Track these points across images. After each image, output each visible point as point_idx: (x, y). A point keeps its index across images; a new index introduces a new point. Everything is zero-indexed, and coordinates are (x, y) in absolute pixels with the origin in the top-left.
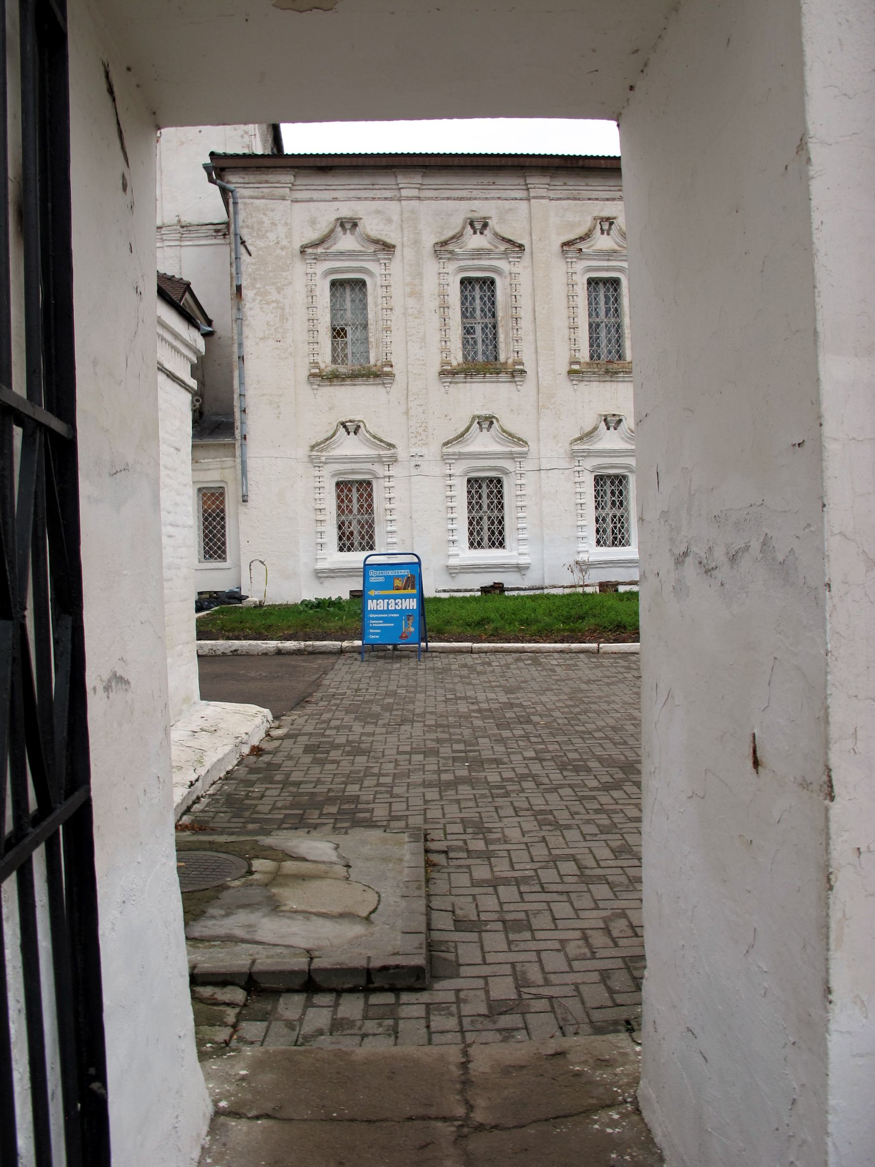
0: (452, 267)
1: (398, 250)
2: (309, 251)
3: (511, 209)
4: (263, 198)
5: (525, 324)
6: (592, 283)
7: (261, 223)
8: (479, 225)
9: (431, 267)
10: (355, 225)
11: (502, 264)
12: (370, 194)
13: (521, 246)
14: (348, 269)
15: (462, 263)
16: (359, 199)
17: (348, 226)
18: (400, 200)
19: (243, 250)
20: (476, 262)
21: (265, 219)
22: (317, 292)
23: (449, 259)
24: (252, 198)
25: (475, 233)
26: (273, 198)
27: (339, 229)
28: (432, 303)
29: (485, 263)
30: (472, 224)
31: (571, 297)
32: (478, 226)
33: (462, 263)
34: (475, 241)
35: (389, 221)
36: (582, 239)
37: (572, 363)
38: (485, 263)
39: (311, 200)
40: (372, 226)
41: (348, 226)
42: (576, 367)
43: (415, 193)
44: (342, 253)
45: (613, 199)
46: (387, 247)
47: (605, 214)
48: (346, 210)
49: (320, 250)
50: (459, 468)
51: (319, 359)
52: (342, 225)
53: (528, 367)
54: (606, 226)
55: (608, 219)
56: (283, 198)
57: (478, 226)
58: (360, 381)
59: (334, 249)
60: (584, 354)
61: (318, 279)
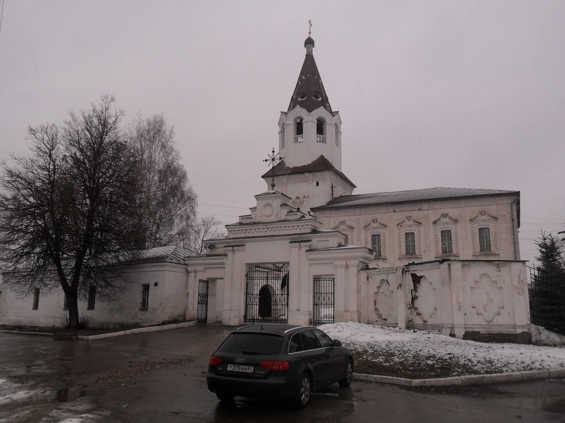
1: (355, 229)
4: (323, 217)
5: (387, 246)
8: (375, 221)
9: (363, 232)
10: (344, 223)
11: (381, 231)
12: (348, 214)
13: (386, 226)
15: (371, 231)
17: (343, 223)
18: (355, 215)
20: (375, 231)
25: (374, 223)
26: (325, 217)
27: (341, 224)
29: (377, 231)
30: (373, 221)
31: (400, 238)
32: (375, 221)
33: (371, 231)
34: (375, 225)
36: (402, 223)
38: (377, 231)
39: (334, 217)
40: (349, 223)
41: (343, 223)
42: (400, 257)
43: (359, 214)
46: (352, 228)
47: (409, 215)
48: (342, 219)
52: (341, 223)
53: (388, 258)
54: (409, 218)
55: (409, 217)
56: (328, 217)
57: (375, 221)
60: (404, 252)
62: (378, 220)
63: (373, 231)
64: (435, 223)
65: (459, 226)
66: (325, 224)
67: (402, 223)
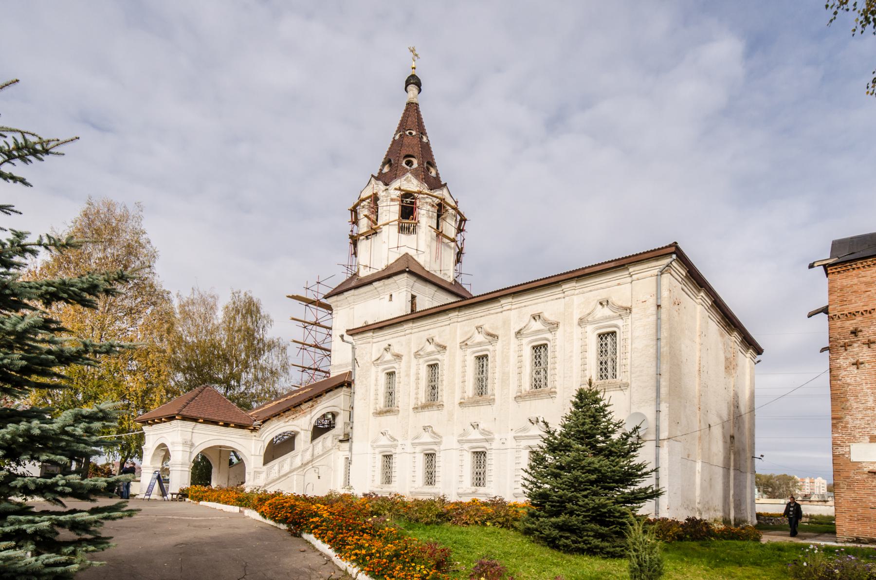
0: (421, 360)
2: (375, 362)
3: (443, 331)
6: (601, 336)
7: (362, 354)
9: (414, 362)
14: (389, 367)
15: (425, 359)
16: (393, 338)
19: (356, 365)
20: (430, 357)
21: (364, 352)
22: (379, 378)
23: (420, 358)
24: (361, 344)
28: (413, 378)
32: (431, 341)
35: (402, 345)
36: (468, 339)
37: (461, 399)
38: (433, 357)
40: (396, 349)
44: (385, 362)
45: (484, 316)
49: (379, 361)
50: (524, 443)
51: (378, 406)
58: (388, 414)
59: (385, 360)
61: (421, 367)
62: (434, 339)
63: (427, 358)
64: (519, 333)
65: (559, 332)
66: (366, 354)
67: (468, 339)
